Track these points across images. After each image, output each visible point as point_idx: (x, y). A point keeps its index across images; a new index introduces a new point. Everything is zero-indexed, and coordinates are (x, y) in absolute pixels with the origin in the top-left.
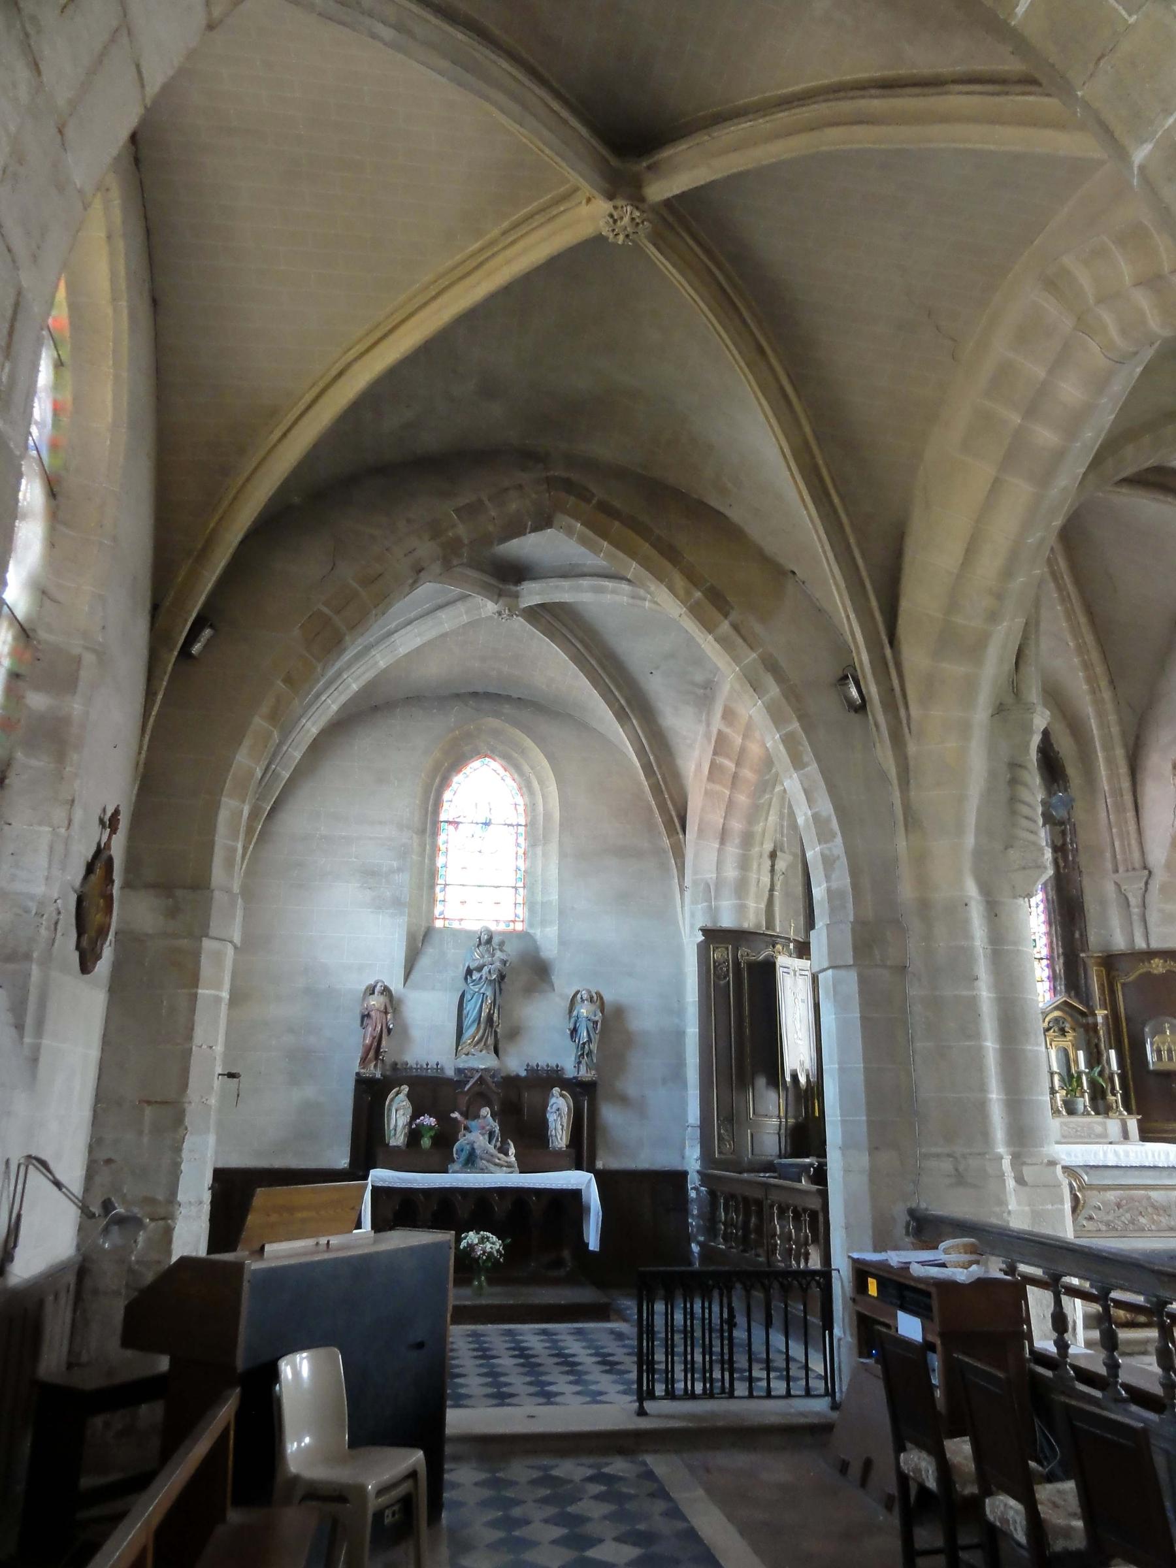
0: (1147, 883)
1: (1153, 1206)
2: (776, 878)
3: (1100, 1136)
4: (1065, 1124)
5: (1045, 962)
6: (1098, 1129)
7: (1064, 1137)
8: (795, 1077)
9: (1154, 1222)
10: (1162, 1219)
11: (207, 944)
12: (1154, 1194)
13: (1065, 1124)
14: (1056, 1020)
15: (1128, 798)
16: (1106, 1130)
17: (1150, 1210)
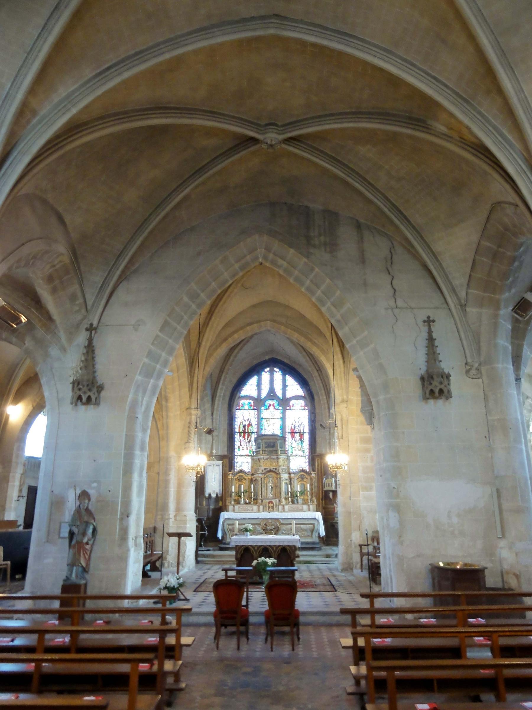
0: (330, 432)
1: (302, 529)
2: (214, 438)
3: (301, 510)
4: (290, 506)
5: (307, 457)
6: (300, 508)
7: (289, 510)
8: (210, 495)
9: (303, 534)
10: (305, 533)
11: (11, 474)
12: (302, 526)
13: (290, 506)
14: (301, 475)
15: (326, 405)
16: (303, 507)
17: (301, 530)
